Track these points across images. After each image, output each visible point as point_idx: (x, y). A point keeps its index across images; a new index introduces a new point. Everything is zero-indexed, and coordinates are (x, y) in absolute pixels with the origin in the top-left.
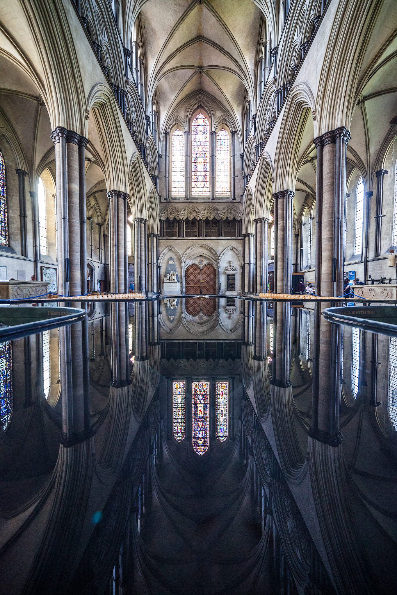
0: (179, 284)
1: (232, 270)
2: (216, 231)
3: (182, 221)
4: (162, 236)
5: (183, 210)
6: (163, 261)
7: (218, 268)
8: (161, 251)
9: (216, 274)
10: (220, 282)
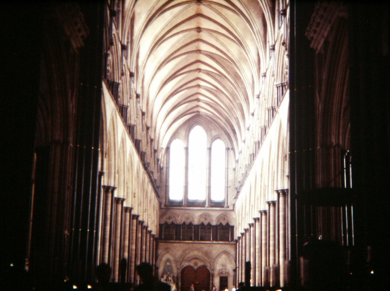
7: (213, 270)
8: (159, 253)
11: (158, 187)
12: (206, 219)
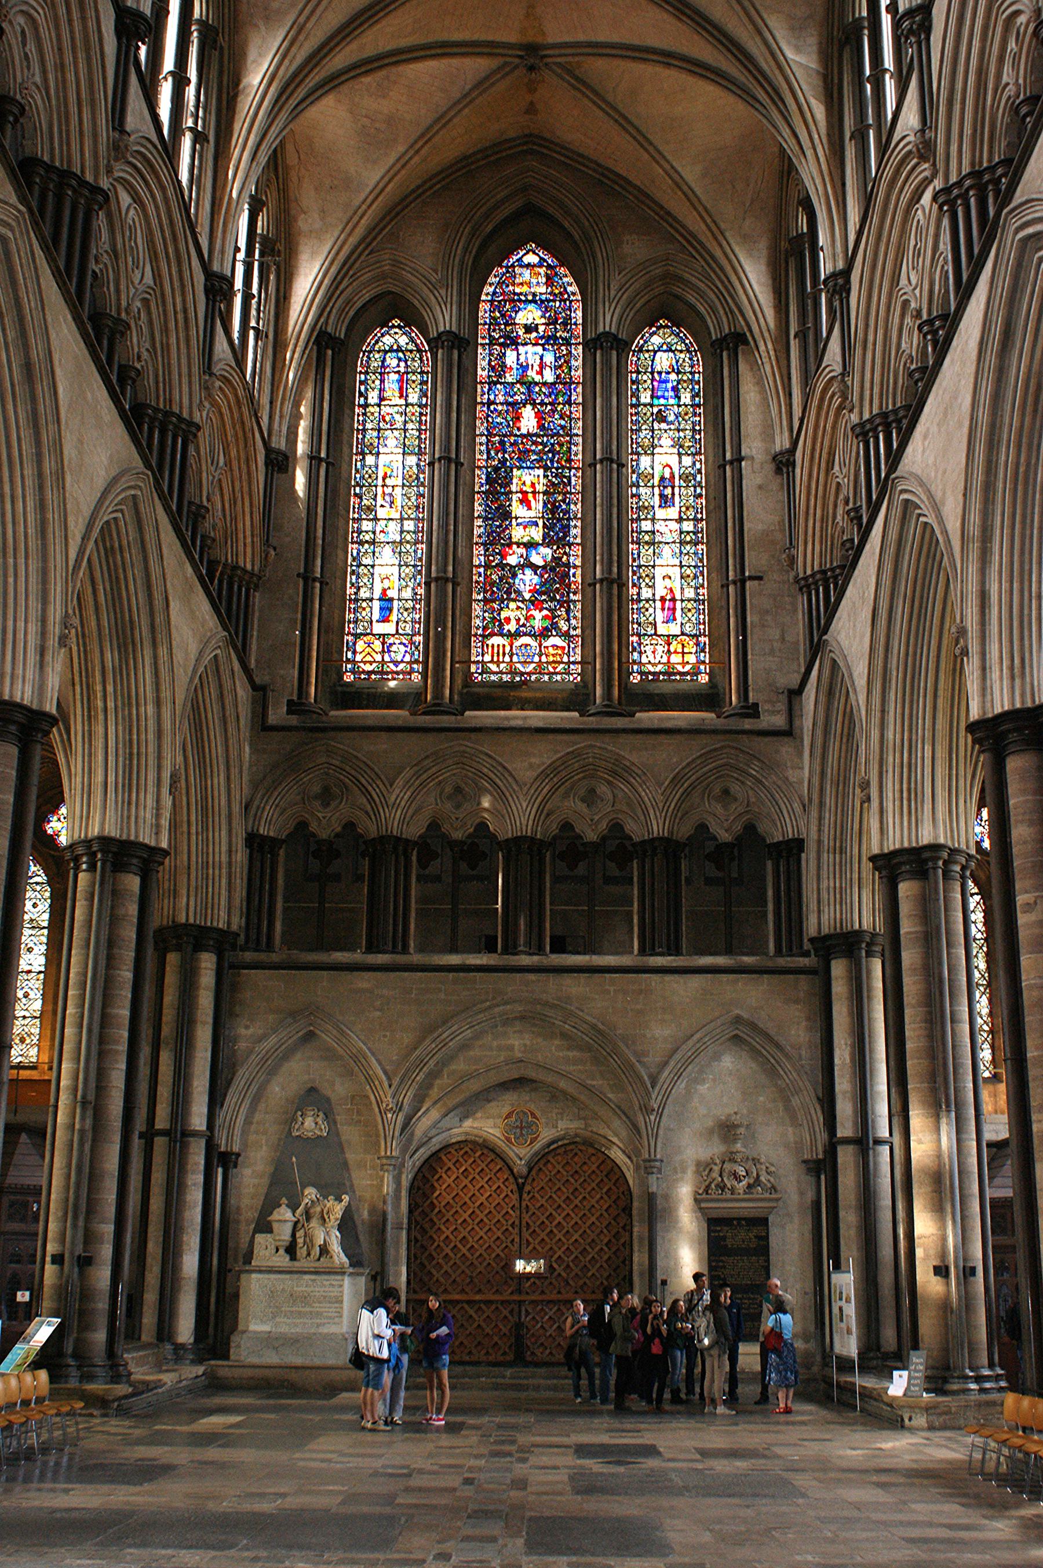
0: (362, 1281)
2: (630, 914)
3: (398, 845)
4: (258, 941)
6: (257, 1117)
8: (242, 1045)
9: (628, 1210)
10: (660, 1277)
11: (253, 581)
12: (591, 797)
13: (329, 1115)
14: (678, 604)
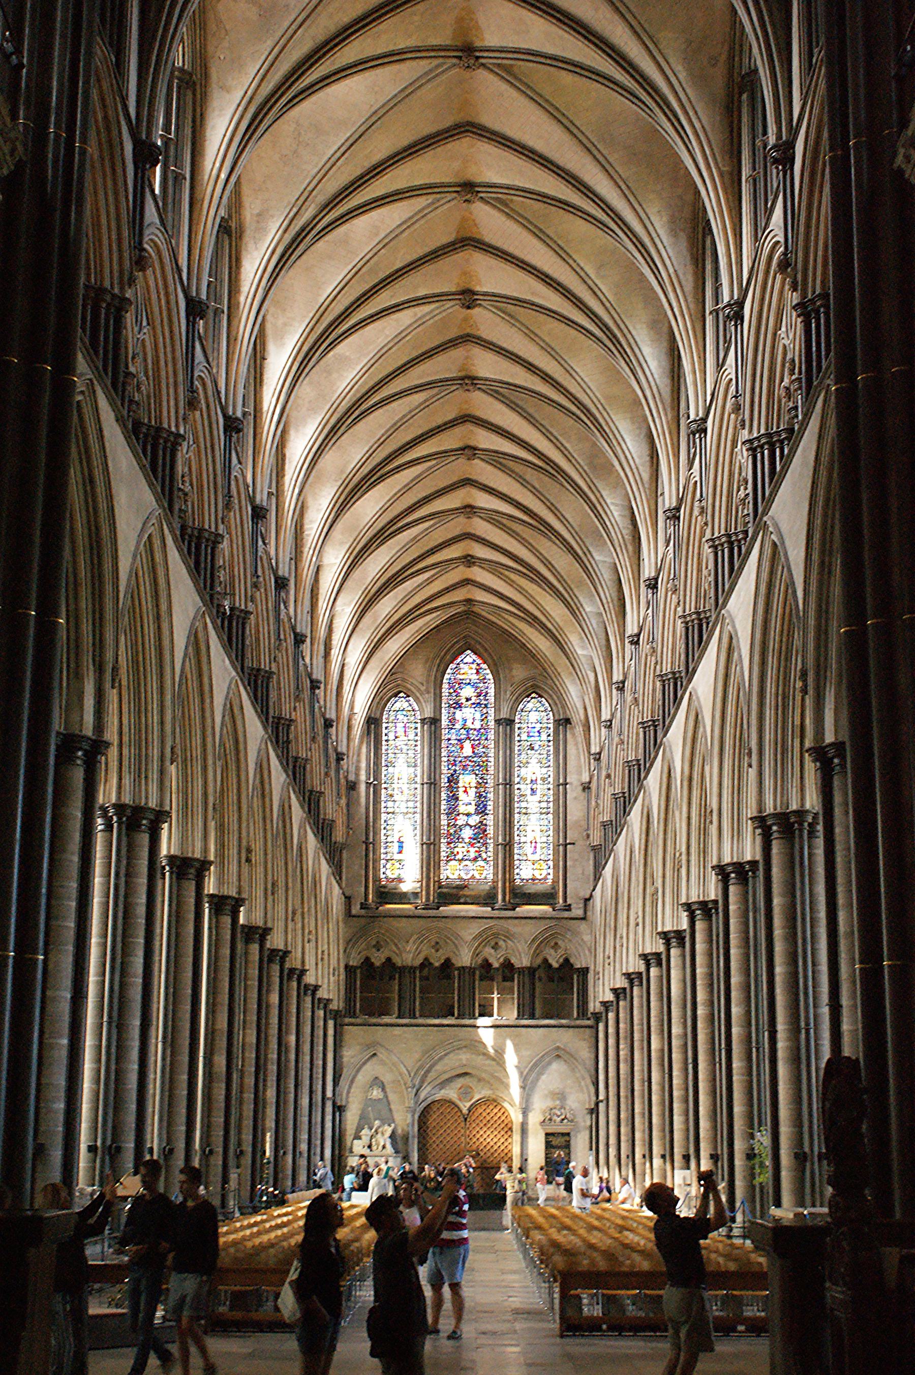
1: (559, 1119)
3: (412, 969)
5: (415, 937)
8: (345, 1060)
11: (343, 846)
12: (496, 947)
13: (383, 1089)
14: (539, 845)
